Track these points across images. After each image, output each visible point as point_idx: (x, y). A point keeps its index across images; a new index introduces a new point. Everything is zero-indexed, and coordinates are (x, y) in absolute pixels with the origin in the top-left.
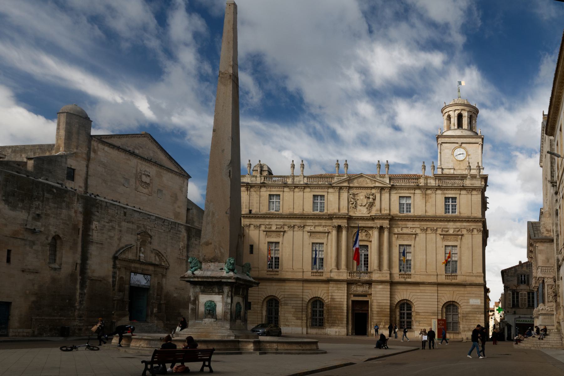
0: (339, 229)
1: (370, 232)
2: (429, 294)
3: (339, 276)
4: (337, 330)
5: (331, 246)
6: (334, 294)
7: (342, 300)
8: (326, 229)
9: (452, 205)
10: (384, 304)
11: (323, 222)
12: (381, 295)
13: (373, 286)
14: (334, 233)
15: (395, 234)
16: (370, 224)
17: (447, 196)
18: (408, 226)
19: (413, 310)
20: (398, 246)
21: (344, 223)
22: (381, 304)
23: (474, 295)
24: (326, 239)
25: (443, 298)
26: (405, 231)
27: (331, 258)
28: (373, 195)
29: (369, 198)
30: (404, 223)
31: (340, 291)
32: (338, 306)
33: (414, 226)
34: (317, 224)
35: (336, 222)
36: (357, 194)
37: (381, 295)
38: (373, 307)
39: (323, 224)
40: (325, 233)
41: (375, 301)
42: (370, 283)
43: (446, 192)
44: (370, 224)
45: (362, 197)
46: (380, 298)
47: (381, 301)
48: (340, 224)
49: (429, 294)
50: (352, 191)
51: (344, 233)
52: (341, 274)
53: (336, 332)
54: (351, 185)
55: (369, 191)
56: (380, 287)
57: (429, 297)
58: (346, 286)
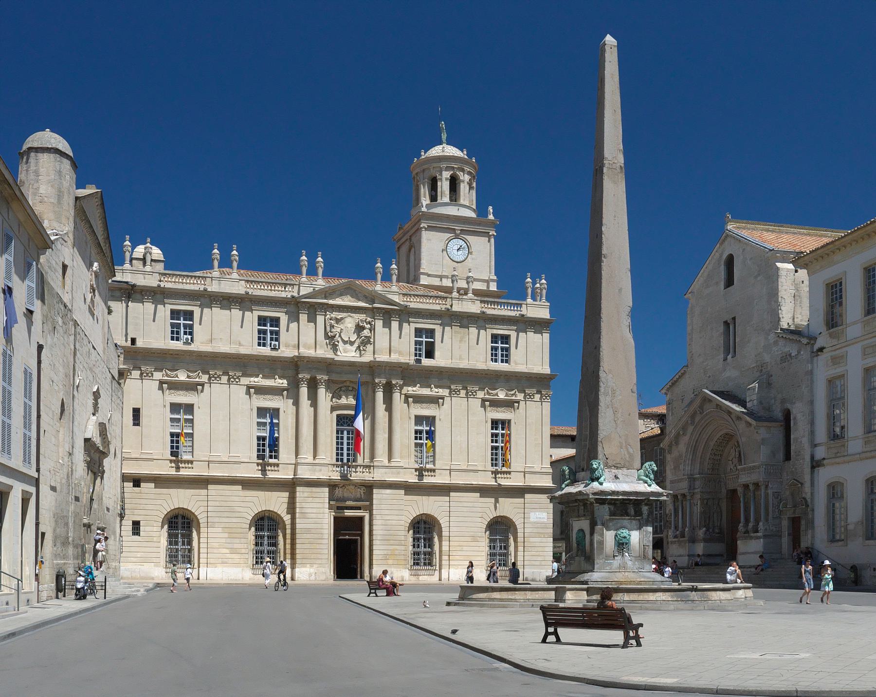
2: (465, 504)
3: (315, 471)
4: (312, 570)
6: (304, 505)
7: (321, 516)
10: (394, 522)
12: (389, 507)
13: (375, 491)
20: (413, 418)
23: (537, 506)
25: (488, 512)
28: (369, 323)
29: (363, 328)
31: (317, 500)
32: (313, 526)
36: (342, 319)
37: (389, 507)
41: (378, 517)
45: (350, 325)
46: (387, 512)
47: (388, 517)
49: (465, 504)
50: (335, 315)
53: (310, 575)
54: (331, 302)
55: (363, 317)
56: (388, 491)
57: (465, 509)
58: (327, 490)
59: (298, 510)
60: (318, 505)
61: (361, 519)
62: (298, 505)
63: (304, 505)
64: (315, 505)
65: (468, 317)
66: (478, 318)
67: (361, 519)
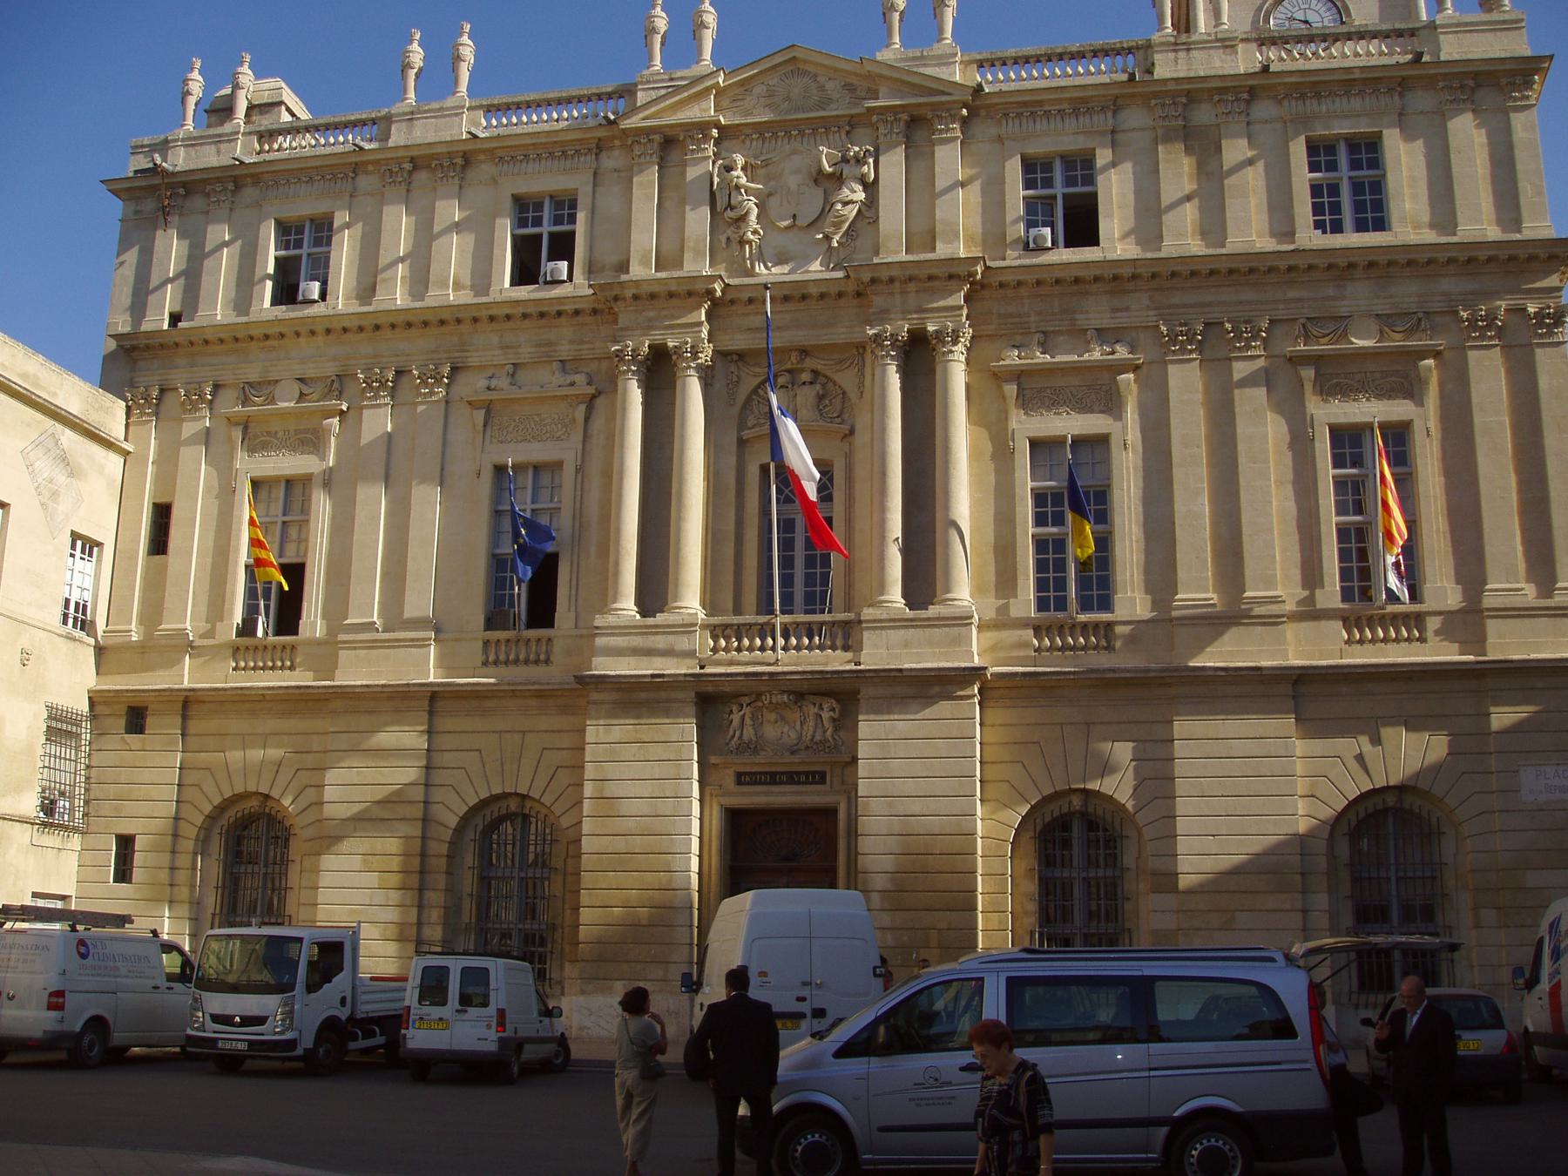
1: (846, 379)
2: (1238, 747)
6: (611, 770)
9: (1357, 187)
12: (918, 767)
17: (1320, 131)
19: (1129, 859)
22: (917, 825)
24: (577, 437)
31: (657, 751)
32: (638, 843)
33: (1123, 320)
37: (918, 767)
38: (865, 845)
39: (565, 351)
42: (845, 696)
43: (1312, 106)
46: (910, 786)
47: (916, 806)
49: (1238, 747)
59: (588, 789)
60: (657, 770)
61: (830, 813)
62: (590, 771)
63: (611, 770)
64: (636, 769)
65: (1222, 90)
66: (1252, 91)
67: (830, 813)
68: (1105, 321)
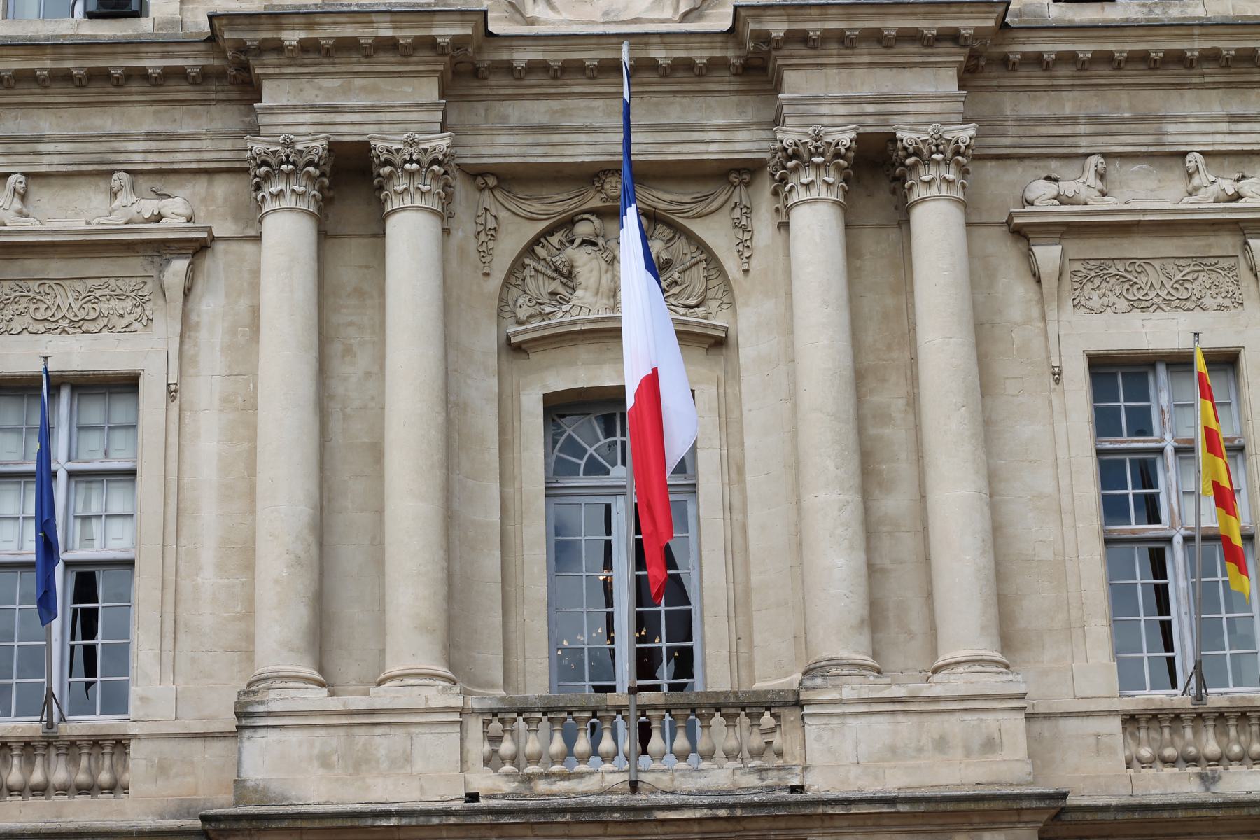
0: (349, 182)
1: (716, 233)
3: (360, 763)
5: (244, 410)
8: (176, 210)
11: (135, 128)
14: (287, 231)
15: (1021, 233)
16: (713, 128)
18: (1176, 136)
21: (396, 114)
26: (1147, 193)
27: (243, 554)
30: (1124, 103)
34: (51, 156)
35: (304, 113)
39: (137, 153)
40: (161, 249)
44: (713, 128)
48: (348, 128)
51: (410, 233)
52: (383, 743)
68: (1222, 139)
